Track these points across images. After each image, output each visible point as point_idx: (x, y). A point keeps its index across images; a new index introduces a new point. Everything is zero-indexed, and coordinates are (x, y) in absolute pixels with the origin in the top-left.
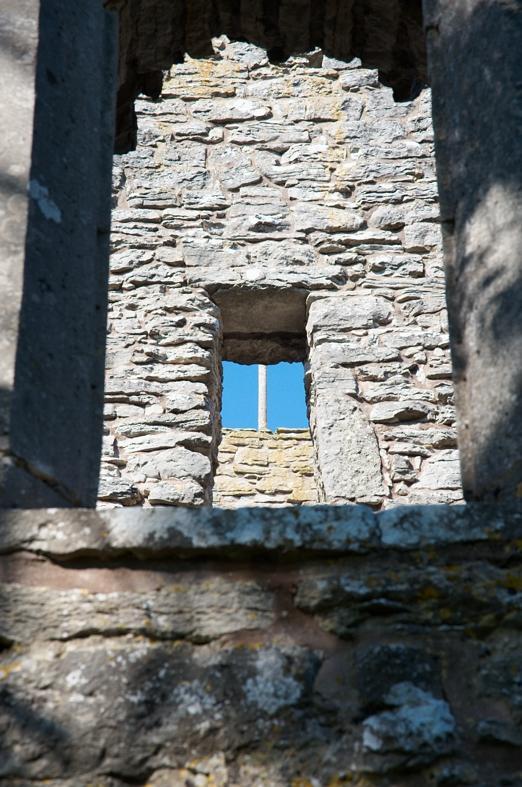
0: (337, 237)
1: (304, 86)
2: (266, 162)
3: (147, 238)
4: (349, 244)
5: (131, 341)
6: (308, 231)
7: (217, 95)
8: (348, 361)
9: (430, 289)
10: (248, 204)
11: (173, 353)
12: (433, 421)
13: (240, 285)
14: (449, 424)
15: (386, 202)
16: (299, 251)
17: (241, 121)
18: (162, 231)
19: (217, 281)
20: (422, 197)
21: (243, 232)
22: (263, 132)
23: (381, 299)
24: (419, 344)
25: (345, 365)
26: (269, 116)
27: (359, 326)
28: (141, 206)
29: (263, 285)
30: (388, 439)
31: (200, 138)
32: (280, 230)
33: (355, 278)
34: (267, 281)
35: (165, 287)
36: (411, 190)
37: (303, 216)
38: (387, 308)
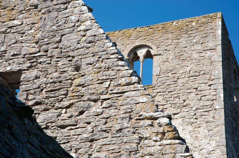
0: (32, 55)
1: (32, 14)
4: (34, 57)
6: (25, 55)
7: (10, 20)
8: (26, 90)
9: (51, 67)
10: (12, 49)
12: (44, 104)
13: (5, 72)
15: (45, 44)
21: (9, 57)
23: (39, 72)
24: (45, 83)
27: (32, 79)
29: (11, 71)
32: (19, 55)
33: (34, 66)
34: (12, 70)
37: (24, 51)
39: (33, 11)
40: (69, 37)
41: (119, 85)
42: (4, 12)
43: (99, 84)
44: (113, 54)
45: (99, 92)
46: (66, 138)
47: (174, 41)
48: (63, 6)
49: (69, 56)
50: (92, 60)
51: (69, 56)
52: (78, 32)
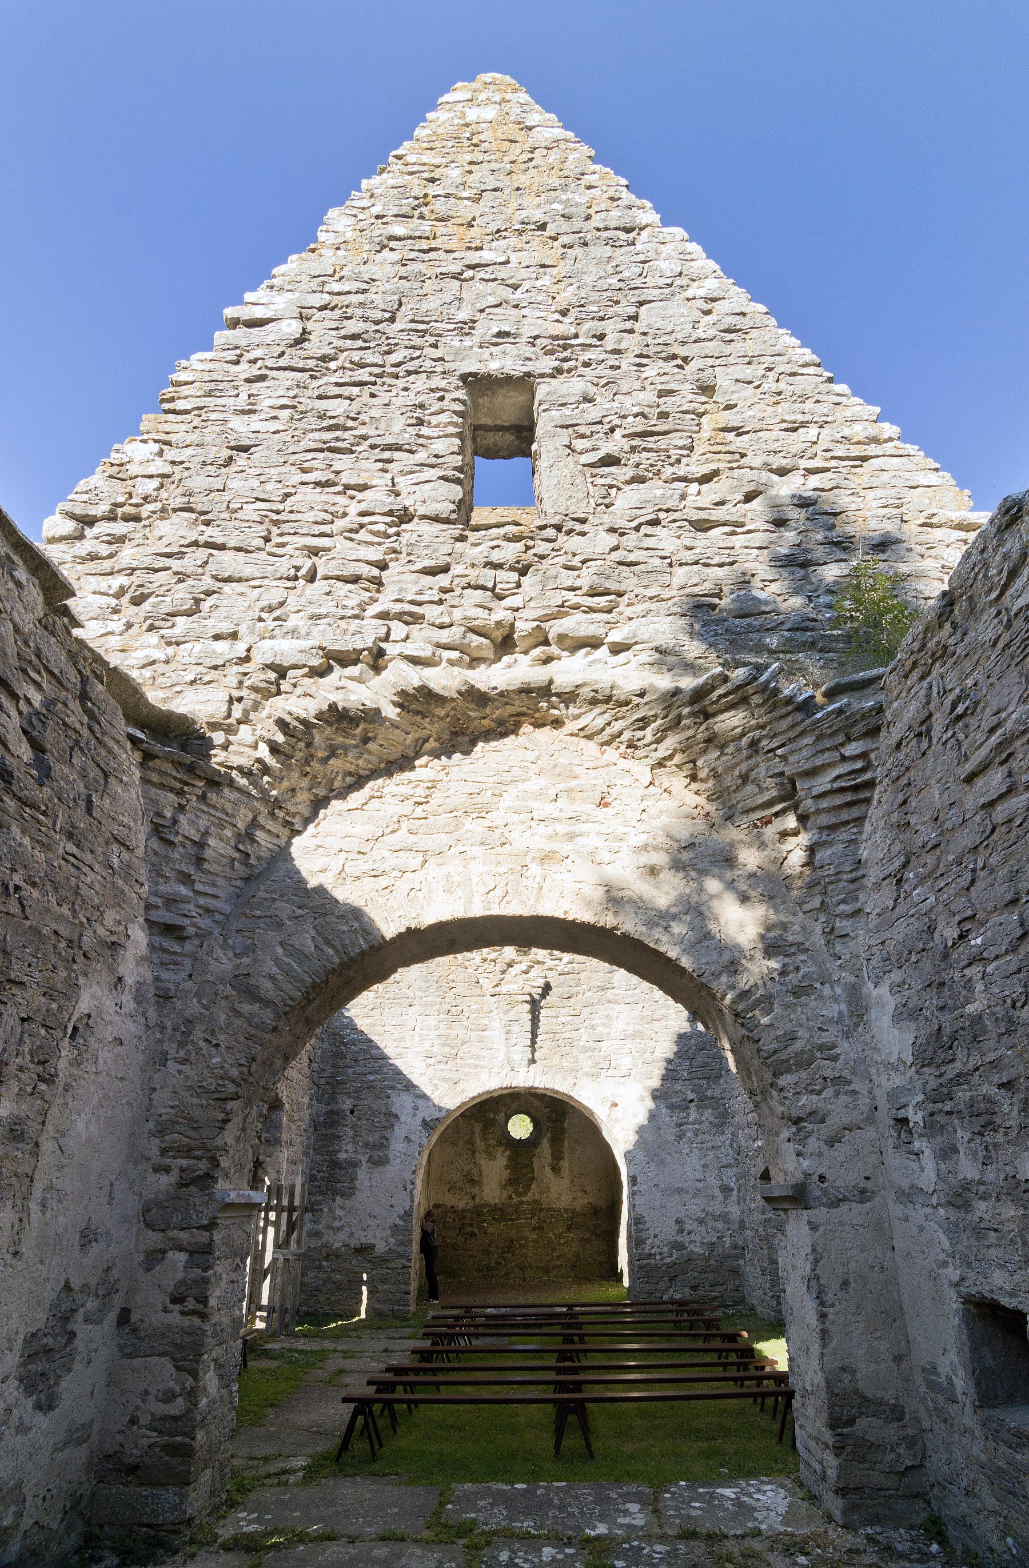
1: (533, 244)
2: (507, 293)
3: (417, 341)
5: (404, 410)
6: (536, 337)
7: (469, 248)
11: (435, 420)
14: (637, 466)
16: (529, 351)
17: (488, 265)
18: (427, 337)
19: (467, 371)
20: (619, 316)
21: (488, 338)
22: (503, 273)
25: (562, 427)
26: (508, 262)
28: (413, 321)
30: (593, 476)
31: (456, 276)
33: (569, 371)
34: (505, 371)
35: (430, 374)
36: (611, 311)
38: (592, 390)
39: (537, 239)
43: (786, 430)
45: (793, 451)
46: (727, 551)
48: (623, 236)
49: (674, 357)
50: (748, 372)
51: (674, 357)
52: (688, 299)
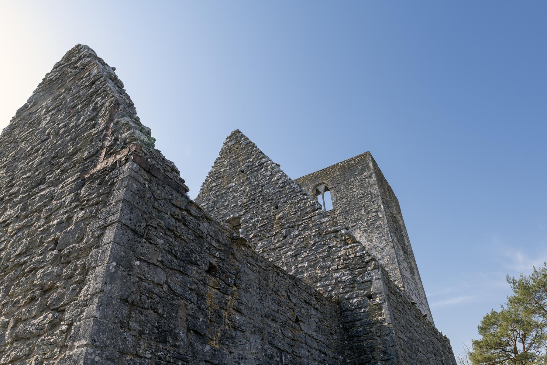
4: (247, 205)
40: (267, 186)
41: (307, 213)
42: (223, 179)
44: (299, 192)
47: (342, 176)
49: (270, 200)
